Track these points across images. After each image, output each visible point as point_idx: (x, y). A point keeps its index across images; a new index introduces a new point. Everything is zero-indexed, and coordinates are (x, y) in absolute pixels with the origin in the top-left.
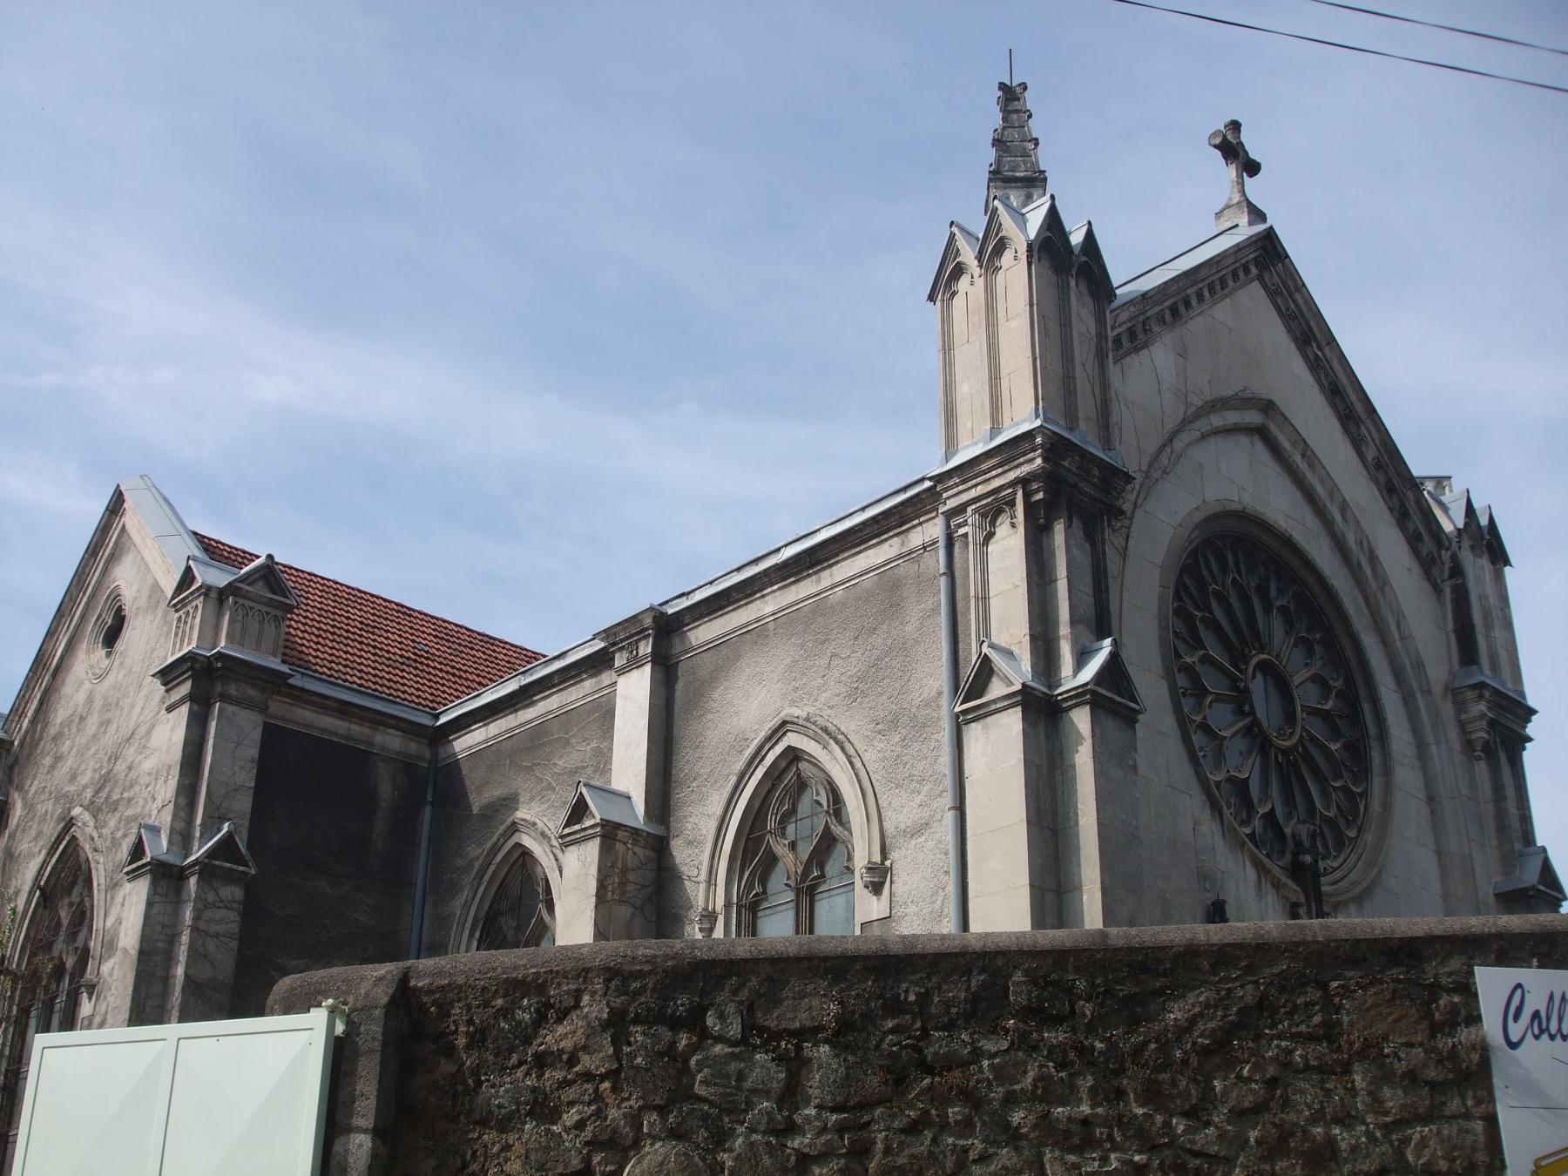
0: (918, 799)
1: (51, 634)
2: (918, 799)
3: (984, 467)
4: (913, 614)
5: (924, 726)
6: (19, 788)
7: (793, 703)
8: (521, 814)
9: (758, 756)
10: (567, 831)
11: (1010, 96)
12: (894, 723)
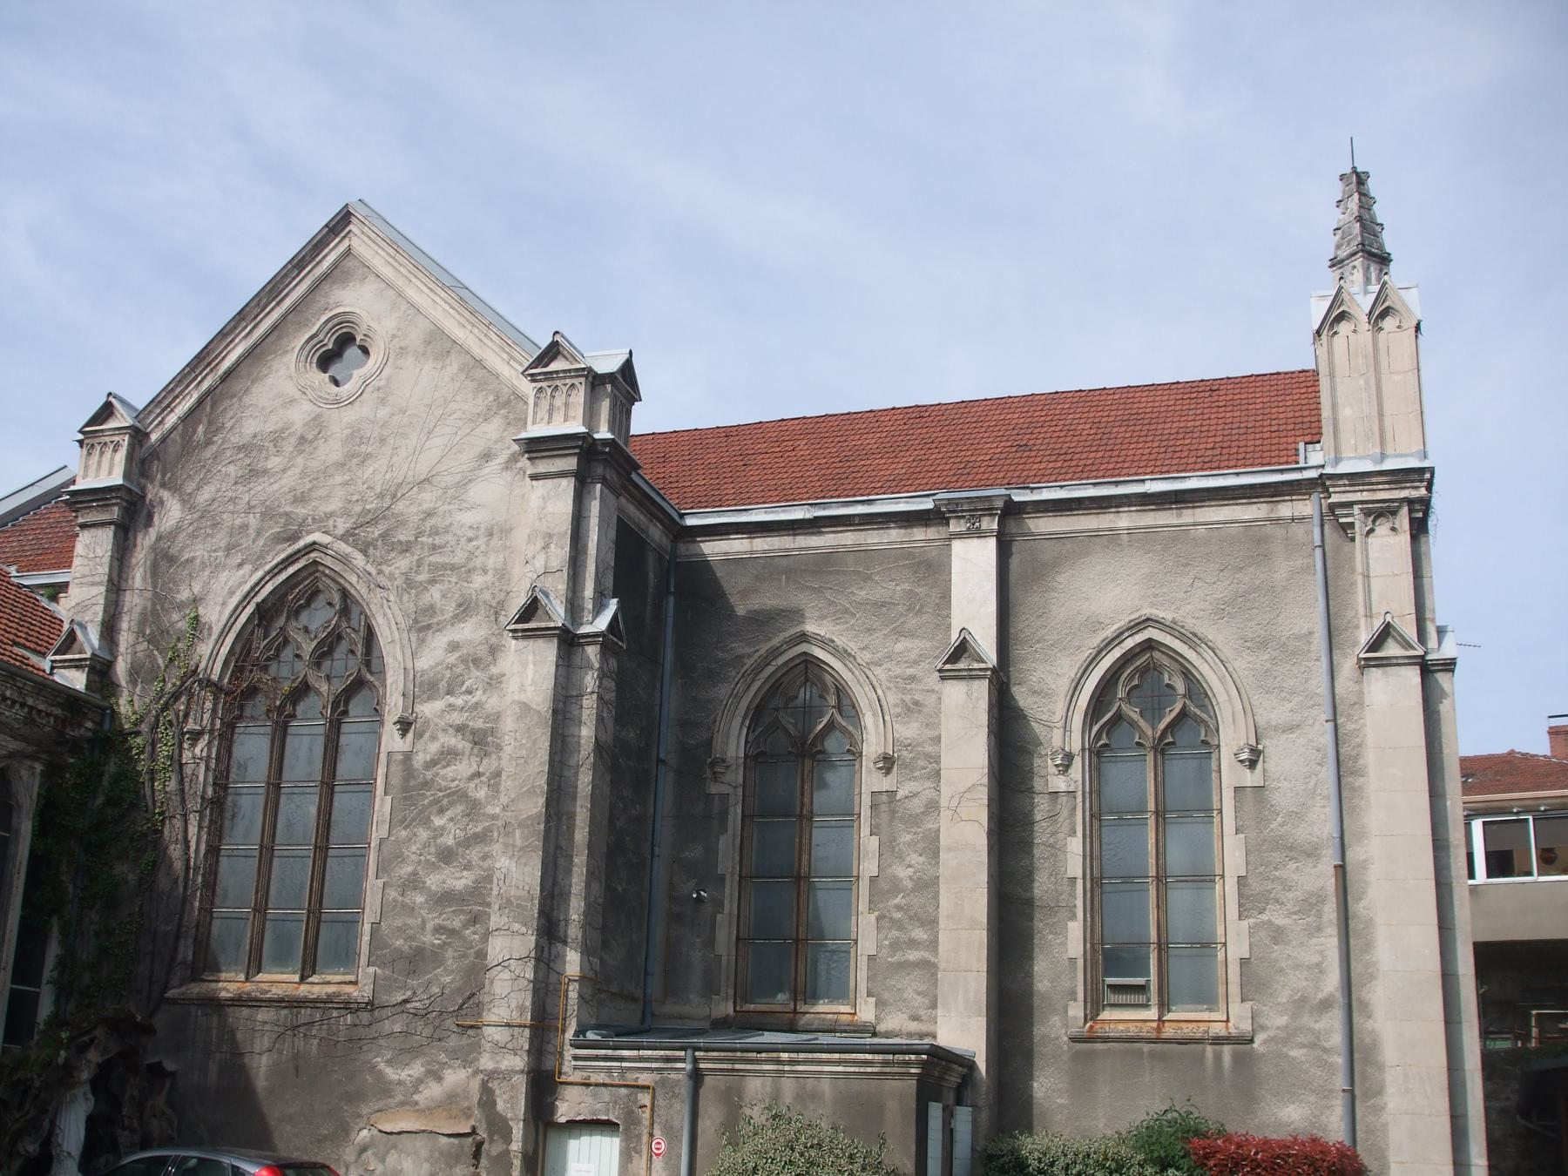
0: (1289, 706)
1: (223, 334)
2: (1289, 706)
3: (1374, 480)
4: (1281, 569)
5: (1294, 653)
6: (173, 486)
7: (1152, 605)
8: (810, 627)
9: (1117, 638)
10: (948, 667)
11: (1359, 180)
12: (1263, 644)
